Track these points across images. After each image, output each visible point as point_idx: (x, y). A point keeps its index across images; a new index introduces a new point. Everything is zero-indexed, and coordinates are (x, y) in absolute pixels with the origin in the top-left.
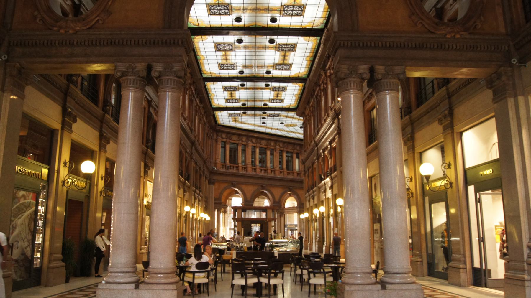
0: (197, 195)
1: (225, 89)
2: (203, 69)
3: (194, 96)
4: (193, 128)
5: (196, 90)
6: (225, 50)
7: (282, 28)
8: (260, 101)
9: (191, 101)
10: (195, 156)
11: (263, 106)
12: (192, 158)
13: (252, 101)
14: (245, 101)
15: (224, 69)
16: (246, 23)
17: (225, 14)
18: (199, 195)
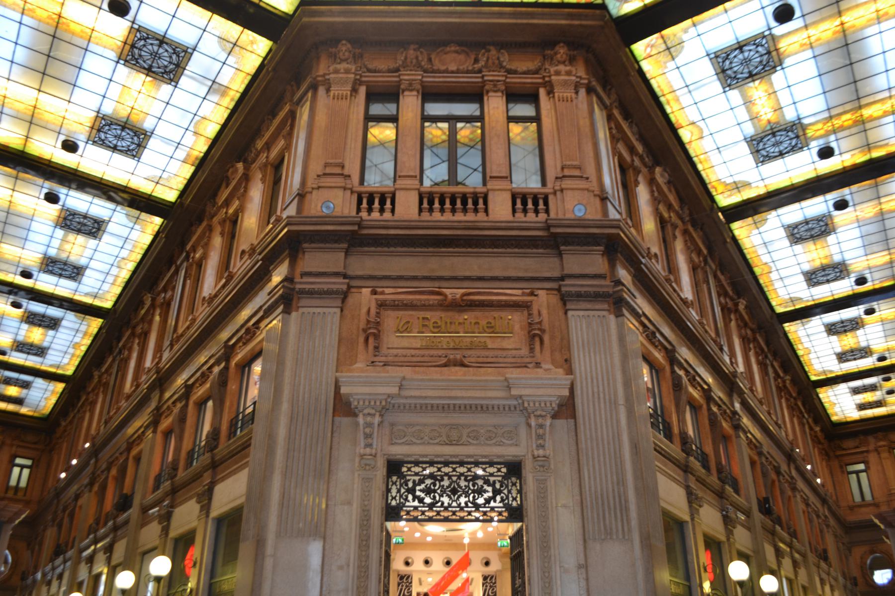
0: (824, 576)
1: (832, 329)
2: (771, 296)
3: (766, 357)
4: (779, 422)
5: (768, 344)
9: (763, 366)
10: (801, 484)
12: (794, 489)
15: (819, 283)
18: (828, 574)
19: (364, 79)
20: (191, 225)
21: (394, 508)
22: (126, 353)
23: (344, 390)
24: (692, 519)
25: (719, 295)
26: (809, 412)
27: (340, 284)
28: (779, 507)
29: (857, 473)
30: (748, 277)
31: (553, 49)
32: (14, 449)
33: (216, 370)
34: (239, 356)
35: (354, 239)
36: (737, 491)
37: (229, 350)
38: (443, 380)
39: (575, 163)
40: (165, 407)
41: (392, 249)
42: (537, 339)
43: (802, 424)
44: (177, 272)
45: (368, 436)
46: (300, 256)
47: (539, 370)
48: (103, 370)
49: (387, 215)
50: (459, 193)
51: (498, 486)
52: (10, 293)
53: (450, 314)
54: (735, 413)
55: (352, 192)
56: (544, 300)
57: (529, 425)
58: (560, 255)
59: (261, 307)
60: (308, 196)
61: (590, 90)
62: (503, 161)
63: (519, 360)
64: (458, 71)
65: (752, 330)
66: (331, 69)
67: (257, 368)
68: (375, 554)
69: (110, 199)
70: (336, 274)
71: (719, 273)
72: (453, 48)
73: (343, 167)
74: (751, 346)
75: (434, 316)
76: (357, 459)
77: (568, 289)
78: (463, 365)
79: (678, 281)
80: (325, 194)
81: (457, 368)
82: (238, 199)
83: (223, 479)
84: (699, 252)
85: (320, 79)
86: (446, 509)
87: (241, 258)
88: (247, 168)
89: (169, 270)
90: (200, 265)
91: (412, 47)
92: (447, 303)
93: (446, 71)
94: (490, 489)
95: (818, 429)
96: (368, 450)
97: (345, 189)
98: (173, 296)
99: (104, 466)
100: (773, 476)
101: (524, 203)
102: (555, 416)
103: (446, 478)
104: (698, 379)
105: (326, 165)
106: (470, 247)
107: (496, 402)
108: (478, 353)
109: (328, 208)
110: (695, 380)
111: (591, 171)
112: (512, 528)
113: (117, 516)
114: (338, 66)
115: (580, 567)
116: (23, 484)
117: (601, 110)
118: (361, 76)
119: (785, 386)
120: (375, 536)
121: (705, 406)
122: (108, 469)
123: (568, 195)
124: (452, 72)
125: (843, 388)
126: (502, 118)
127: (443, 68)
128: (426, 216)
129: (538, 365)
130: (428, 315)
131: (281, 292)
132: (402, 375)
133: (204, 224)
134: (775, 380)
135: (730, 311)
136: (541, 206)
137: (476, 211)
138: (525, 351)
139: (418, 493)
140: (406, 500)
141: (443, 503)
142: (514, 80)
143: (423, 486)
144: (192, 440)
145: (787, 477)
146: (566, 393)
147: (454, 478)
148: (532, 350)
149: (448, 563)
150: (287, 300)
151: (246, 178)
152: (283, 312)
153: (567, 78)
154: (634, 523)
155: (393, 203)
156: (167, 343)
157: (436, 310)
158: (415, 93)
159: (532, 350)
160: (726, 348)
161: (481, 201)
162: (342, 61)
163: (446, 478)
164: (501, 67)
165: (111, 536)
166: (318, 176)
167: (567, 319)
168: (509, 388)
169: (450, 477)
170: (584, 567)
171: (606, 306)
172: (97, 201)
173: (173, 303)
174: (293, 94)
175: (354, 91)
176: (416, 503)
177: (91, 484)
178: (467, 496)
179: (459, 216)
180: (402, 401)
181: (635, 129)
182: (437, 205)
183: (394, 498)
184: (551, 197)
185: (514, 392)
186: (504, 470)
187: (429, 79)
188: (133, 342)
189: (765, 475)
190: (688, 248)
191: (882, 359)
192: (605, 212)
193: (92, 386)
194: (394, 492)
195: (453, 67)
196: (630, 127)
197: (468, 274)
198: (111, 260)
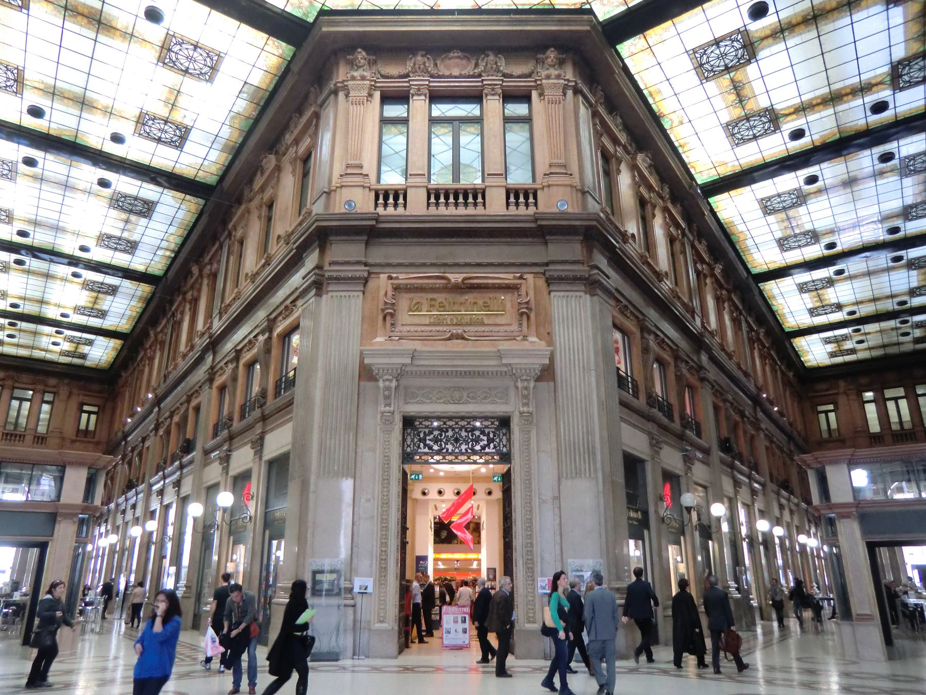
1: (803, 288)
2: (747, 258)
3: (741, 313)
4: (750, 371)
5: (743, 301)
6: (784, 209)
7: (905, 119)
8: (887, 297)
10: (765, 424)
11: (896, 307)
12: (758, 429)
13: (870, 301)
14: (853, 304)
15: (791, 249)
16: (815, 137)
17: (766, 133)
19: (378, 85)
20: (231, 207)
21: (408, 454)
22: (179, 316)
24: (653, 459)
25: (695, 263)
26: (781, 360)
27: (361, 271)
28: (742, 446)
29: (826, 412)
30: (726, 245)
31: (544, 54)
32: (81, 397)
33: (261, 338)
34: (280, 328)
35: (371, 232)
36: (699, 434)
37: (271, 323)
38: (447, 352)
39: (560, 161)
40: (219, 366)
41: (405, 240)
42: (525, 317)
43: (773, 371)
44: (221, 247)
45: (387, 397)
46: (328, 246)
47: (526, 342)
48: (159, 329)
49: (400, 210)
50: (461, 189)
51: (491, 435)
52: (70, 264)
53: (453, 295)
54: (701, 368)
55: (370, 190)
56: (532, 283)
57: (517, 388)
58: (546, 243)
59: (296, 289)
60: (333, 193)
61: (577, 91)
62: (499, 158)
63: (509, 334)
64: (461, 76)
65: (728, 291)
66: (349, 75)
67: (295, 339)
68: (395, 489)
69: (158, 184)
70: (358, 263)
71: (696, 243)
72: (456, 54)
73: (362, 167)
74: (726, 305)
75: (441, 297)
76: (379, 416)
77: (551, 273)
78: (464, 338)
79: (654, 256)
80: (346, 194)
81: (459, 341)
82: (272, 188)
83: (272, 430)
84: (677, 226)
85: (339, 85)
86: (450, 454)
87: (278, 243)
88: (278, 160)
89: (214, 244)
90: (241, 242)
91: (420, 53)
92: (450, 286)
93: (450, 76)
94: (485, 438)
95: (791, 374)
96: (387, 408)
97: (364, 187)
98: (218, 269)
99: (167, 414)
100: (738, 418)
101: (517, 197)
102: (538, 379)
103: (450, 430)
104: (666, 340)
105: (348, 166)
106: (470, 237)
107: (490, 369)
108: (476, 329)
109: (350, 205)
110: (663, 341)
111: (574, 168)
112: (503, 468)
113: (182, 457)
114: (356, 74)
115: (554, 498)
116: (92, 427)
117: (587, 109)
118: (376, 82)
119: (759, 339)
120: (396, 476)
121: (673, 364)
122: (171, 416)
123: (554, 189)
124: (456, 77)
125: (815, 337)
126: (499, 121)
127: (447, 73)
128: (433, 210)
130: (435, 296)
131: (313, 278)
132: (413, 348)
133: (243, 207)
134: (748, 333)
135: (705, 276)
136: (531, 200)
137: (475, 204)
138: (515, 327)
139: (428, 442)
140: (419, 447)
141: (447, 450)
142: (510, 83)
143: (432, 436)
144: (244, 395)
145: (752, 419)
146: (548, 362)
147: (457, 430)
148: (520, 325)
149: (458, 493)
150: (318, 285)
151: (278, 168)
152: (316, 295)
153: (555, 81)
154: (599, 465)
156: (216, 312)
157: (442, 292)
158: (423, 97)
159: (520, 325)
160: (698, 310)
161: (480, 196)
162: (359, 67)
163: (450, 430)
164: (499, 71)
165: (178, 473)
166: (341, 176)
167: (550, 299)
168: (501, 357)
169: (453, 429)
170: (557, 498)
171: (583, 288)
172: (145, 185)
173: (219, 278)
174: (316, 97)
175: (370, 95)
176: (426, 450)
177: (156, 429)
178: (467, 443)
179: (461, 211)
180: (415, 369)
181: (619, 120)
182: (442, 200)
183: (408, 446)
184: (539, 193)
185: (504, 361)
186: (497, 423)
187: (436, 84)
188: (184, 307)
189: (728, 418)
190: (667, 224)
191: (852, 313)
192: (584, 205)
193: (149, 343)
194: (409, 441)
195: (456, 72)
196: (614, 120)
197: (468, 261)
198: (161, 235)
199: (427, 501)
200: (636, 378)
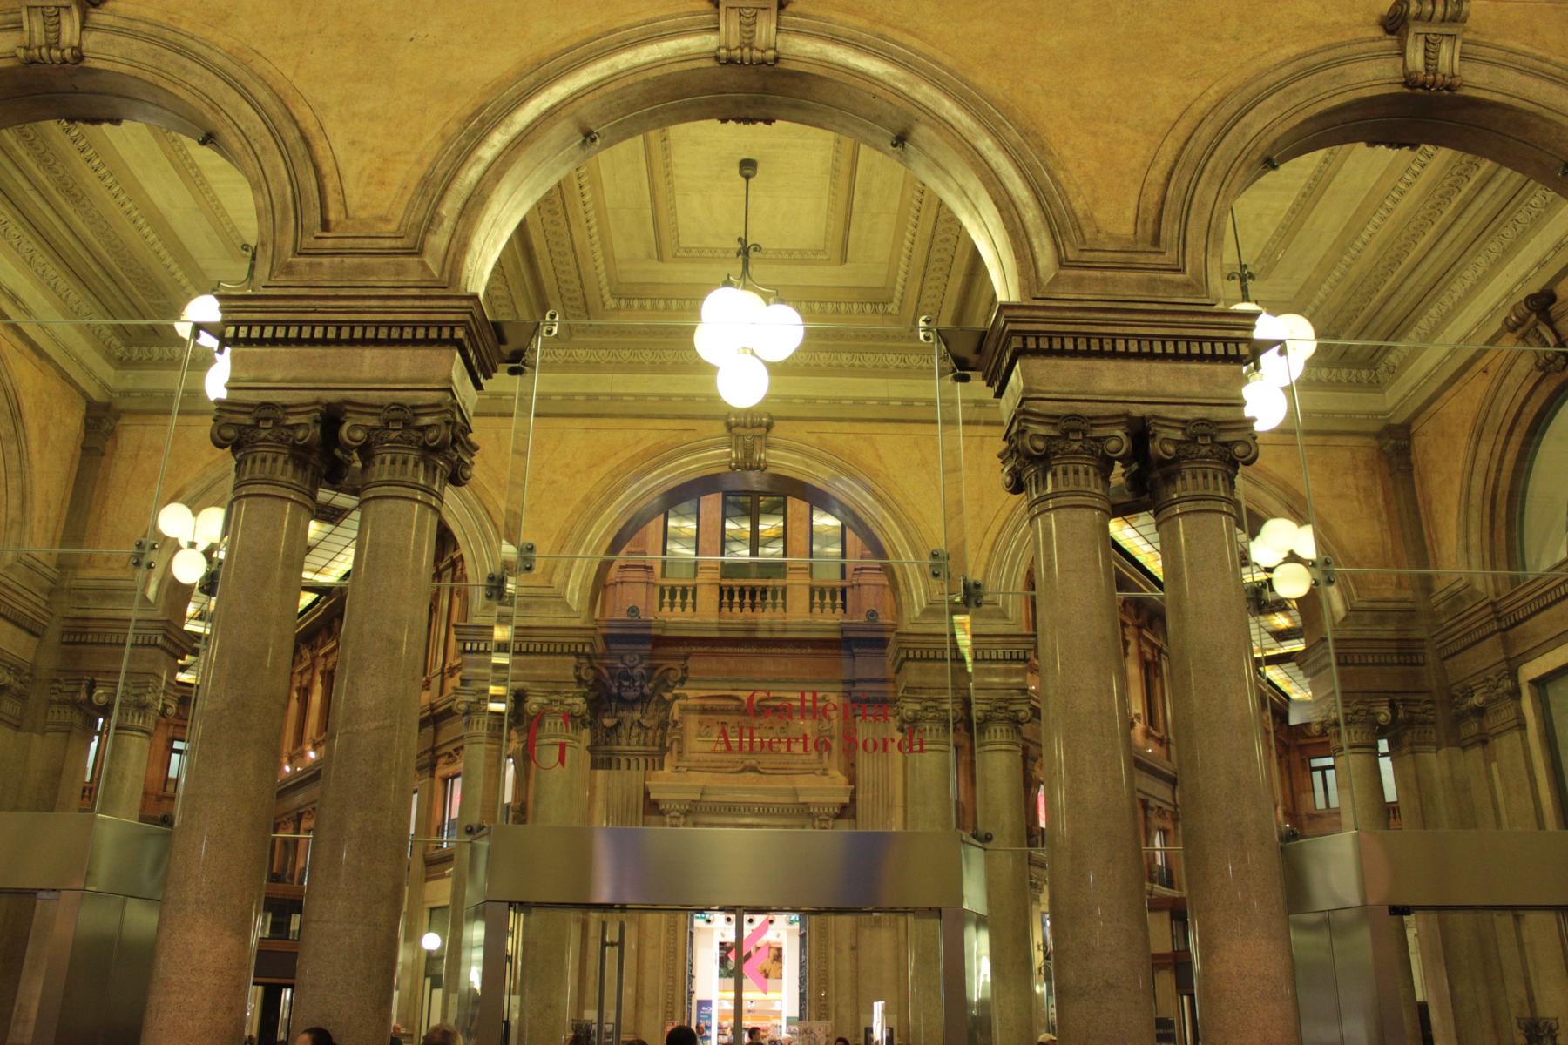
23: (652, 796)
29: (1323, 769)
40: (443, 750)
49: (689, 609)
58: (853, 656)
65: (1139, 627)
81: (753, 775)
101: (822, 597)
102: (838, 817)
128: (726, 609)
129: (825, 773)
130: (726, 718)
132: (701, 783)
146: (847, 800)
155: (694, 597)
170: (853, 948)
185: (801, 799)
199: (712, 931)
200: (962, 799)
